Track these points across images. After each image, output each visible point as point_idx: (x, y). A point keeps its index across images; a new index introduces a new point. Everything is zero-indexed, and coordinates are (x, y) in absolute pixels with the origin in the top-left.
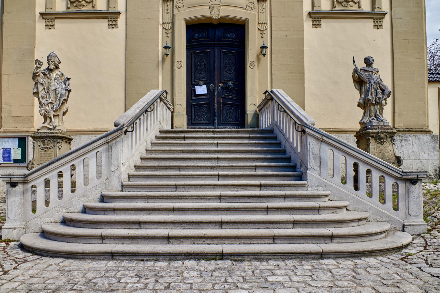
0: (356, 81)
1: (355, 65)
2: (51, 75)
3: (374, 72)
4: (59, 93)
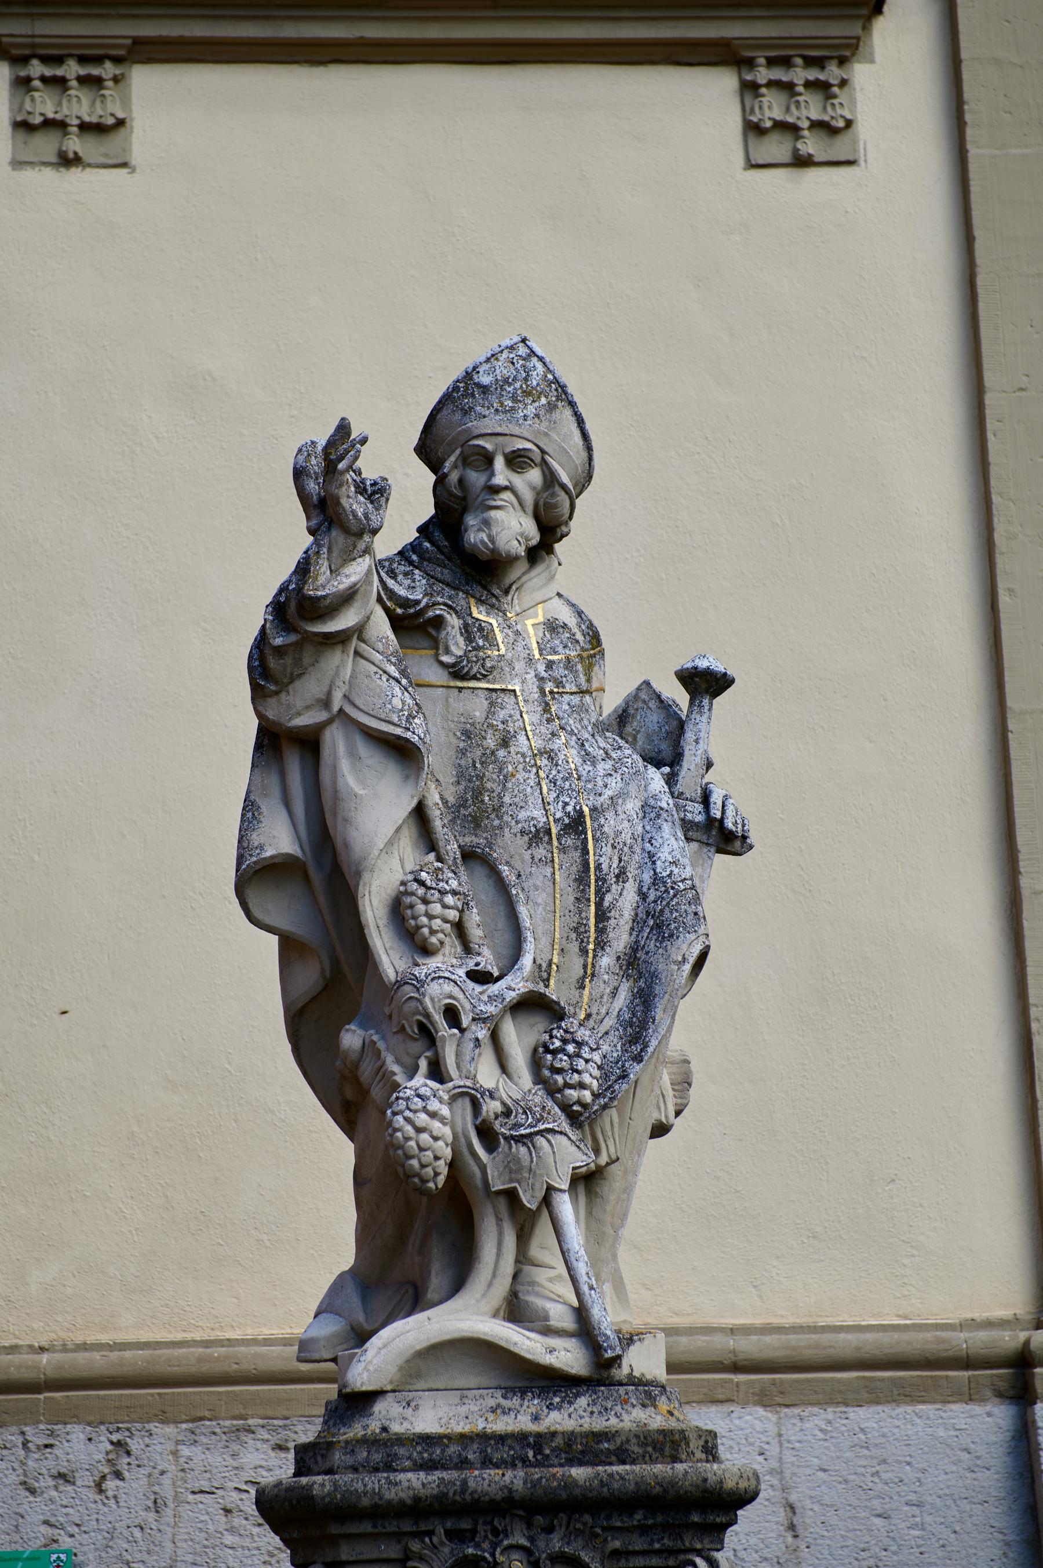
2: (488, 636)
4: (621, 876)
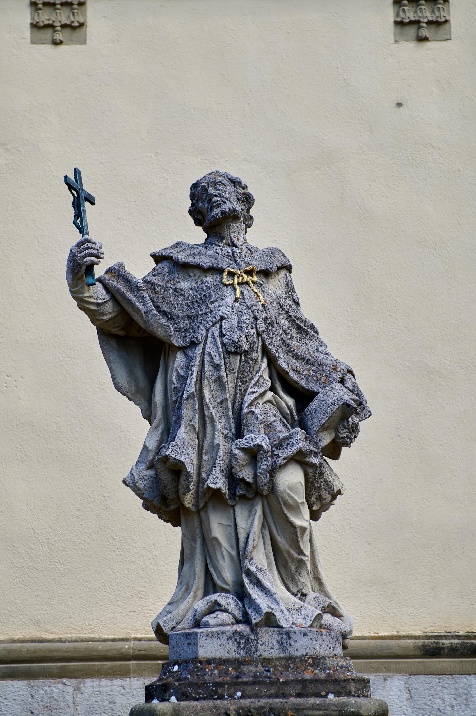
0: (116, 337)
1: (81, 230)
3: (231, 274)
